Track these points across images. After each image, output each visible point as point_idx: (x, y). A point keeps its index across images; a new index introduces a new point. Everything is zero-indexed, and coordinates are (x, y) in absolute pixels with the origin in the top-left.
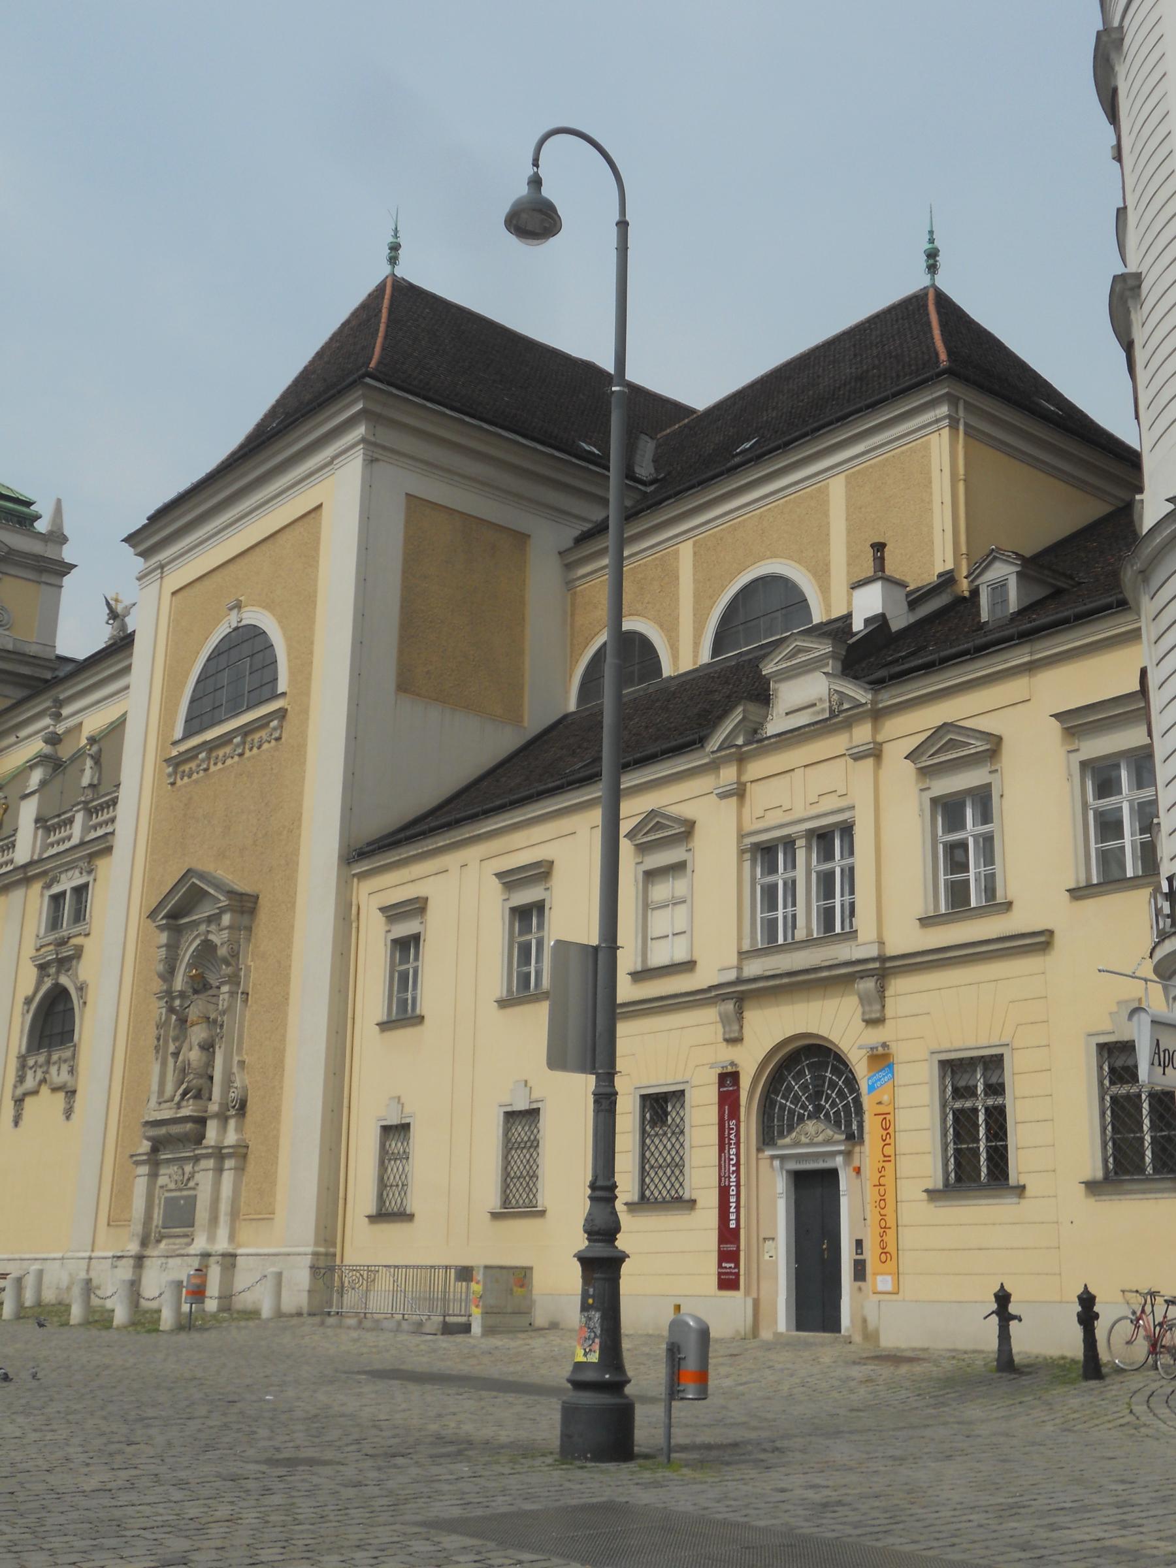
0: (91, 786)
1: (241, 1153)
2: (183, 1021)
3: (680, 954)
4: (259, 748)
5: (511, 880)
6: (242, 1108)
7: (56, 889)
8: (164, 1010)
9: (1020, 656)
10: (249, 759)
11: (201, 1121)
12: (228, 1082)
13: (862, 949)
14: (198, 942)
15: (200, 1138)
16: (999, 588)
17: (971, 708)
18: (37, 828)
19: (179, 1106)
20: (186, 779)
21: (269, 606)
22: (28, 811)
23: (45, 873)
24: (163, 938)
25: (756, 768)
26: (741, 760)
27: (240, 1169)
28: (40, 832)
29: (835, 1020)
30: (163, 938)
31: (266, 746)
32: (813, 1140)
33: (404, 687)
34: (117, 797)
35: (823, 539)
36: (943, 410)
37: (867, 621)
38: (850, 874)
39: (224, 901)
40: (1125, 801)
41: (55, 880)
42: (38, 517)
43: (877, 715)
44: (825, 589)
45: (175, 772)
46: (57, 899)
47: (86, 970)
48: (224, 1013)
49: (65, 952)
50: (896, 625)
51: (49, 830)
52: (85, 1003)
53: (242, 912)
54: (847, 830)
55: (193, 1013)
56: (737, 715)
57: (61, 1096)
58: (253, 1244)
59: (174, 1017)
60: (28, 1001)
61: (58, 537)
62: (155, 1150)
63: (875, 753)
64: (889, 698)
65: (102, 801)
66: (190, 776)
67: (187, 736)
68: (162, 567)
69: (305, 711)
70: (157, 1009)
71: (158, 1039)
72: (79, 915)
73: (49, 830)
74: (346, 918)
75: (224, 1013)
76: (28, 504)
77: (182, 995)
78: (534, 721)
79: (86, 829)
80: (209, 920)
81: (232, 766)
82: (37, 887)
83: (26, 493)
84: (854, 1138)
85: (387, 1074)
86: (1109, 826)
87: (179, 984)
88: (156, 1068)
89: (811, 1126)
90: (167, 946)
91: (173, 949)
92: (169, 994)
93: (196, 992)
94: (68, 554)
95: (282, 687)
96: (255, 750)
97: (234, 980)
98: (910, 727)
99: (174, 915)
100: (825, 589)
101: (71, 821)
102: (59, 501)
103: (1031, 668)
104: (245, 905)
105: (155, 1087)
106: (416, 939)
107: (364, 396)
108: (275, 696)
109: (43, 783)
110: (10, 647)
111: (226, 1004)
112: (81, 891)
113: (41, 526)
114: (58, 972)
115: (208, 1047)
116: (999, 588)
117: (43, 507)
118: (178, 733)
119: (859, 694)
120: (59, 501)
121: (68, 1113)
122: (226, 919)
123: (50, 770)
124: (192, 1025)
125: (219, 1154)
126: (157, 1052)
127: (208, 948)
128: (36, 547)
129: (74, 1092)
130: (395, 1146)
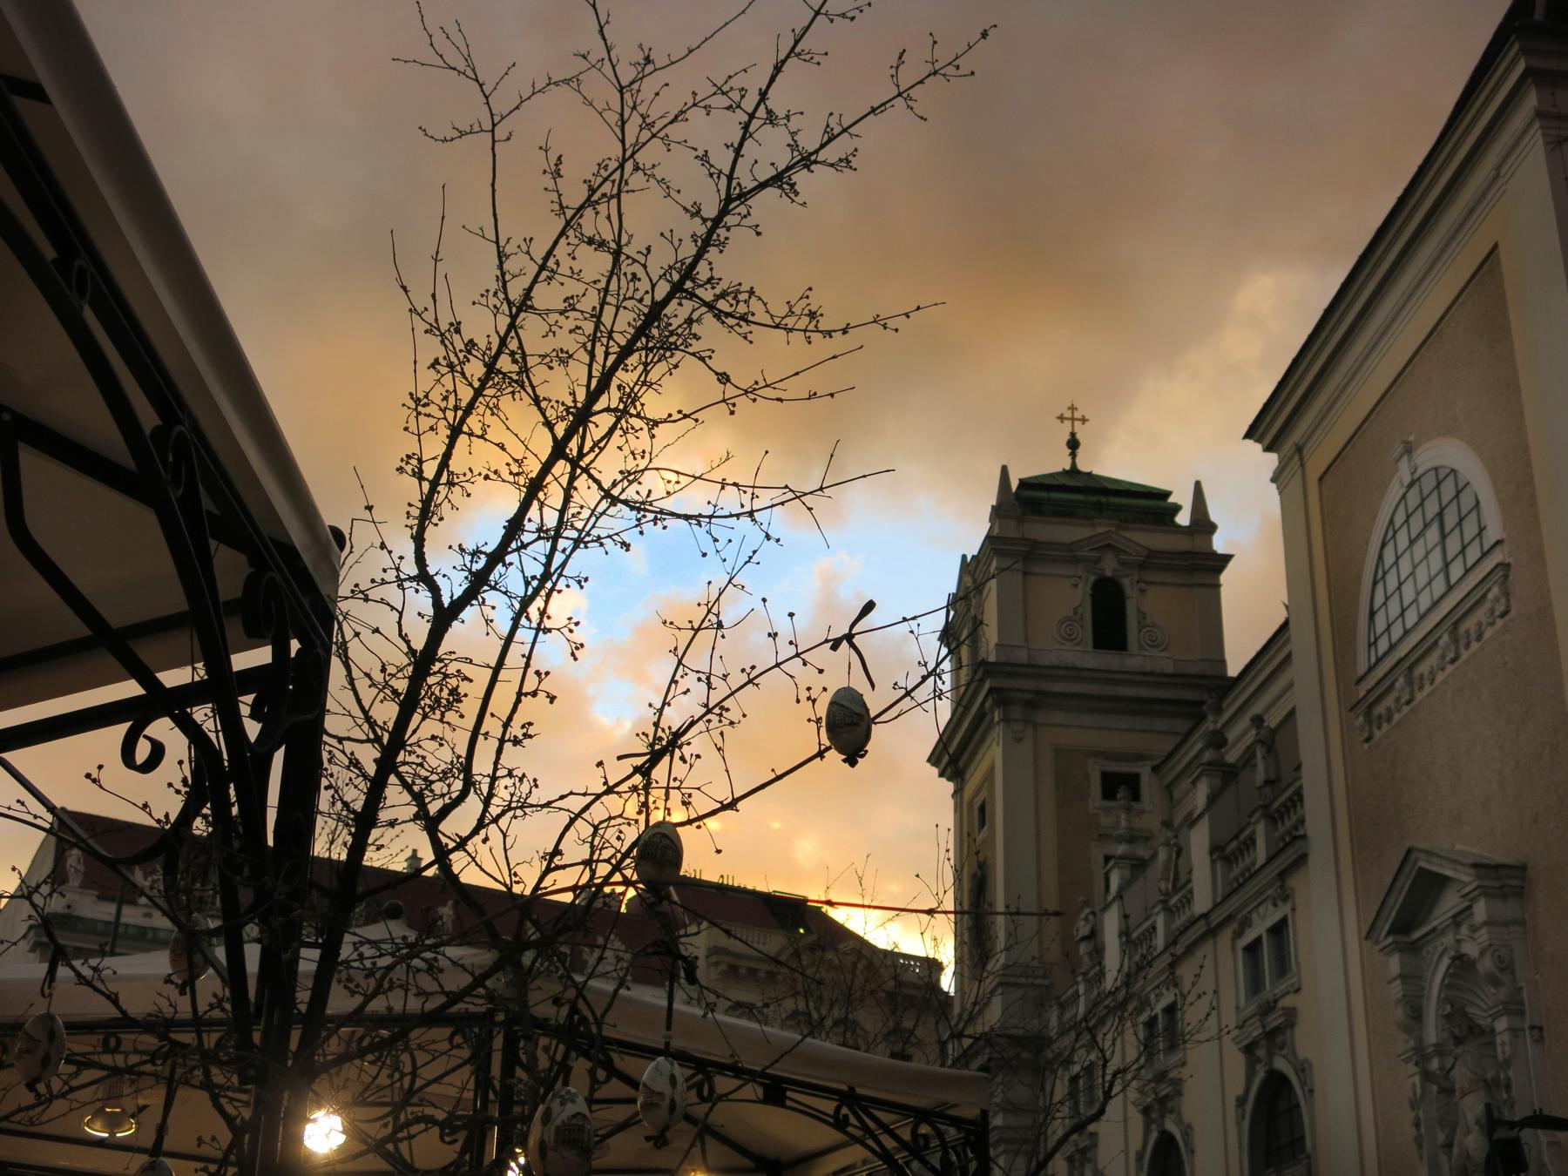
0: (1267, 782)
2: (1447, 1091)
4: (1479, 638)
7: (1249, 936)
8: (1417, 1079)
10: (1467, 662)
14: (1446, 961)
18: (1213, 862)
20: (1385, 727)
22: (1199, 841)
23: (1230, 918)
24: (1394, 964)
28: (1219, 866)
30: (1394, 964)
31: (1489, 633)
34: (1301, 787)
41: (1246, 924)
42: (1177, 508)
45: (1368, 720)
46: (1253, 949)
47: (1304, 1042)
48: (1507, 1063)
49: (1274, 1020)
51: (1229, 861)
52: (1311, 1091)
53: (1504, 897)
55: (1461, 1075)
59: (1435, 1088)
60: (1241, 1101)
61: (1203, 525)
66: (1389, 720)
68: (1299, 449)
70: (1410, 1078)
71: (1417, 1125)
72: (1283, 965)
73: (1229, 861)
75: (1507, 1063)
76: (1165, 495)
77: (1440, 1050)
80: (1457, 921)
81: (1445, 682)
82: (1226, 936)
87: (1432, 1033)
90: (1402, 976)
91: (1412, 979)
92: (1421, 1055)
93: (1459, 1041)
94: (1219, 544)
96: (1474, 646)
97: (1514, 1007)
99: (1402, 927)
101: (1252, 841)
102: (1198, 485)
107: (1524, 51)
109: (1212, 799)
110: (1170, 670)
111: (1507, 1048)
112: (1279, 930)
113: (1183, 519)
114: (1270, 1054)
117: (1182, 497)
120: (1198, 485)
122: (1480, 910)
123: (1218, 782)
124: (1464, 1095)
126: (1420, 1146)
127: (1462, 963)
128: (1182, 544)
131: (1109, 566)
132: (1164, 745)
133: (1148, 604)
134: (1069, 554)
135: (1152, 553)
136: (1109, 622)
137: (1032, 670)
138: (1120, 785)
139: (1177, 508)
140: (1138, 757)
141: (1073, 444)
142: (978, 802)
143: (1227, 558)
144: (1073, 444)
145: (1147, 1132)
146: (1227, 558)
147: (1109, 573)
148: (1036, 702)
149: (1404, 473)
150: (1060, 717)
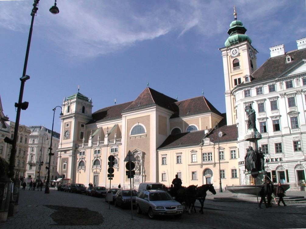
3: (196, 161)
5: (177, 154)
9: (226, 143)
13: (213, 162)
16: (220, 134)
17: (222, 145)
19: (137, 171)
21: (143, 123)
25: (204, 147)
26: (202, 147)
29: (211, 167)
32: (208, 175)
33: (159, 133)
35: (199, 123)
36: (210, 114)
37: (206, 133)
40: (233, 153)
42: (89, 100)
43: (214, 145)
44: (199, 128)
50: (209, 134)
54: (211, 154)
56: (201, 143)
61: (91, 102)
63: (214, 148)
64: (215, 144)
67: (131, 134)
68: (126, 116)
69: (149, 135)
76: (87, 98)
78: (168, 135)
79: (116, 142)
83: (88, 97)
84: (212, 175)
86: (232, 155)
89: (208, 174)
94: (92, 104)
98: (217, 146)
100: (199, 128)
103: (227, 143)
106: (165, 157)
108: (144, 133)
109: (108, 136)
113: (89, 101)
115: (140, 166)
116: (220, 134)
117: (90, 99)
118: (130, 134)
119: (212, 143)
121: (118, 171)
128: (89, 104)
129: (119, 169)
132: (87, 123)
133: (87, 109)
135: (88, 104)
136: (83, 111)
138: (83, 126)
139: (89, 100)
140: (84, 123)
141: (79, 90)
142: (68, 123)
143: (93, 106)
144: (79, 90)
145: (94, 159)
146: (93, 106)
147: (84, 106)
149: (138, 124)
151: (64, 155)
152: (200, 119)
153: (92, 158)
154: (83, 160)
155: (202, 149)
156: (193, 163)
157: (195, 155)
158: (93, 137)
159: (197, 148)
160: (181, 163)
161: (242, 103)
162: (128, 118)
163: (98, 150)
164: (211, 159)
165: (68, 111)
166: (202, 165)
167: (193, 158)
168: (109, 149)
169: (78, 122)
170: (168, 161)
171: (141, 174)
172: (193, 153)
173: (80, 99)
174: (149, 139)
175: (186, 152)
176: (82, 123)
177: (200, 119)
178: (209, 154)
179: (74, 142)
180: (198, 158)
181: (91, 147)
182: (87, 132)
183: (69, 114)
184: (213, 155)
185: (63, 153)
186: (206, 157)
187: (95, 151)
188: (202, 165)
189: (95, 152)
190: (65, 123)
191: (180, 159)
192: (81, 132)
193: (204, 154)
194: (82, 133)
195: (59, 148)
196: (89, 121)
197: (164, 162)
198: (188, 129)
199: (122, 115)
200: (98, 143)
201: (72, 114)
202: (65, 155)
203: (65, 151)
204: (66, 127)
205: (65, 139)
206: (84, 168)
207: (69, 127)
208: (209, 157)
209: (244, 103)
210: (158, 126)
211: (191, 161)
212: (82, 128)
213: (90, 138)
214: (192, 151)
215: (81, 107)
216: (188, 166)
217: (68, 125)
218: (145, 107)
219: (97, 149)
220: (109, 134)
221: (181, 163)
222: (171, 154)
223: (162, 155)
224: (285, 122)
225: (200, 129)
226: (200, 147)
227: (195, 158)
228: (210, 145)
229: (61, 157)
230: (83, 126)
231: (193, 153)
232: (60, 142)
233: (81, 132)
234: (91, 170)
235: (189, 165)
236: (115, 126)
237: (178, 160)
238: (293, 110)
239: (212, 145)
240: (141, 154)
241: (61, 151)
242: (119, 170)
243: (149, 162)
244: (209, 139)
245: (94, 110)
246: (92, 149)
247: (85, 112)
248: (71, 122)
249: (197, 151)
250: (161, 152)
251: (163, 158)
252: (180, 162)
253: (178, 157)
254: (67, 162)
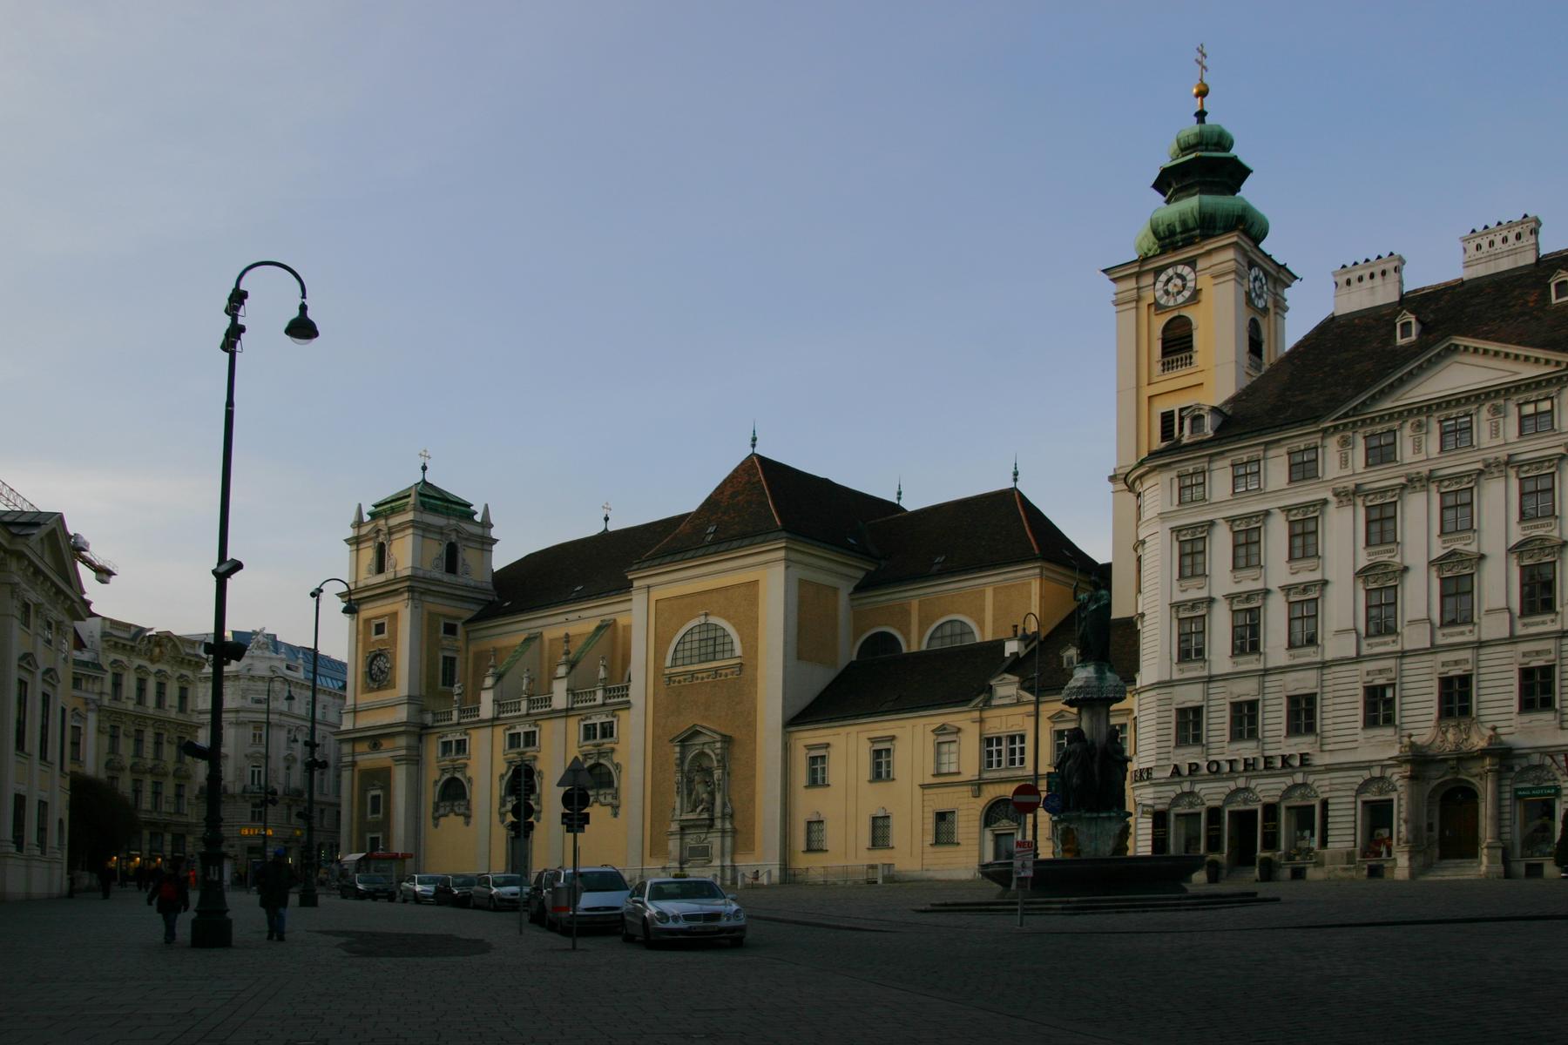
1: (734, 831)
3: (953, 769)
5: (873, 740)
6: (732, 816)
11: (712, 819)
12: (724, 805)
15: (711, 826)
25: (986, 714)
26: (981, 710)
27: (733, 837)
38: (1022, 750)
39: (718, 737)
57: (609, 809)
58: (746, 863)
62: (682, 829)
65: (618, 688)
74: (786, 748)
79: (605, 698)
85: (808, 803)
88: (678, 800)
95: (738, 651)
104: (727, 740)
105: (678, 805)
106: (823, 757)
109: (568, 674)
115: (712, 794)
118: (668, 662)
119: (1028, 697)
121: (616, 815)
125: (723, 831)
127: (702, 754)
130: (815, 827)
131: (454, 538)
132: (468, 615)
134: (440, 531)
136: (451, 561)
137: (424, 579)
138: (450, 630)
148: (426, 592)
150: (431, 599)
151: (370, 759)
152: (989, 593)
153: (501, 767)
154: (458, 775)
155: (981, 721)
156: (942, 780)
157: (953, 747)
158: (499, 677)
159: (962, 719)
160: (889, 778)
161: (1164, 530)
162: (657, 594)
163: (527, 734)
164: (1022, 761)
165: (380, 568)
166: (979, 785)
167: (945, 759)
168: (575, 727)
169: (430, 613)
170: (836, 770)
171: (718, 824)
172: (942, 739)
173: (434, 510)
174: (753, 682)
175: (912, 735)
176: (445, 616)
177: (989, 593)
178: (1012, 739)
179: (411, 700)
180: (966, 757)
181: (493, 722)
182: (471, 655)
183: (381, 578)
184: (1029, 744)
185: (362, 747)
186: (999, 753)
187: (512, 736)
188: (978, 785)
189: (514, 739)
190: (367, 621)
191: (888, 764)
192: (445, 658)
193: (989, 741)
194: (450, 663)
195: (343, 728)
196: (478, 608)
197: (819, 776)
198: (931, 638)
199: (631, 581)
200: (524, 705)
201: (396, 580)
202: (376, 756)
203: (375, 740)
204: (375, 638)
205: (371, 690)
206: (462, 810)
207: (385, 636)
208: (1013, 752)
209: (1173, 530)
210: (794, 631)
211: (931, 769)
212: (447, 641)
213: (489, 682)
214: (941, 730)
215: (437, 549)
216: (918, 791)
217: (380, 629)
218: (735, 544)
219: (521, 729)
220: (572, 665)
221: (889, 778)
222: (847, 744)
223: (810, 748)
224: (1342, 608)
225: (989, 637)
226: (976, 714)
227: (954, 758)
228: (1019, 702)
229: (354, 764)
230: (450, 630)
231: (942, 739)
232: (350, 701)
233: (445, 658)
234: (496, 817)
235: (924, 786)
236: (599, 628)
237: (878, 765)
238: (1384, 558)
239: (1028, 703)
240: (718, 745)
241: (354, 740)
242: (622, 811)
243: (754, 776)
244: (1016, 679)
245: (502, 557)
246: (499, 731)
247: (460, 569)
248: (394, 616)
249: (959, 730)
250: (809, 736)
251: (813, 760)
252: (888, 773)
253: (878, 753)
254: (387, 787)
